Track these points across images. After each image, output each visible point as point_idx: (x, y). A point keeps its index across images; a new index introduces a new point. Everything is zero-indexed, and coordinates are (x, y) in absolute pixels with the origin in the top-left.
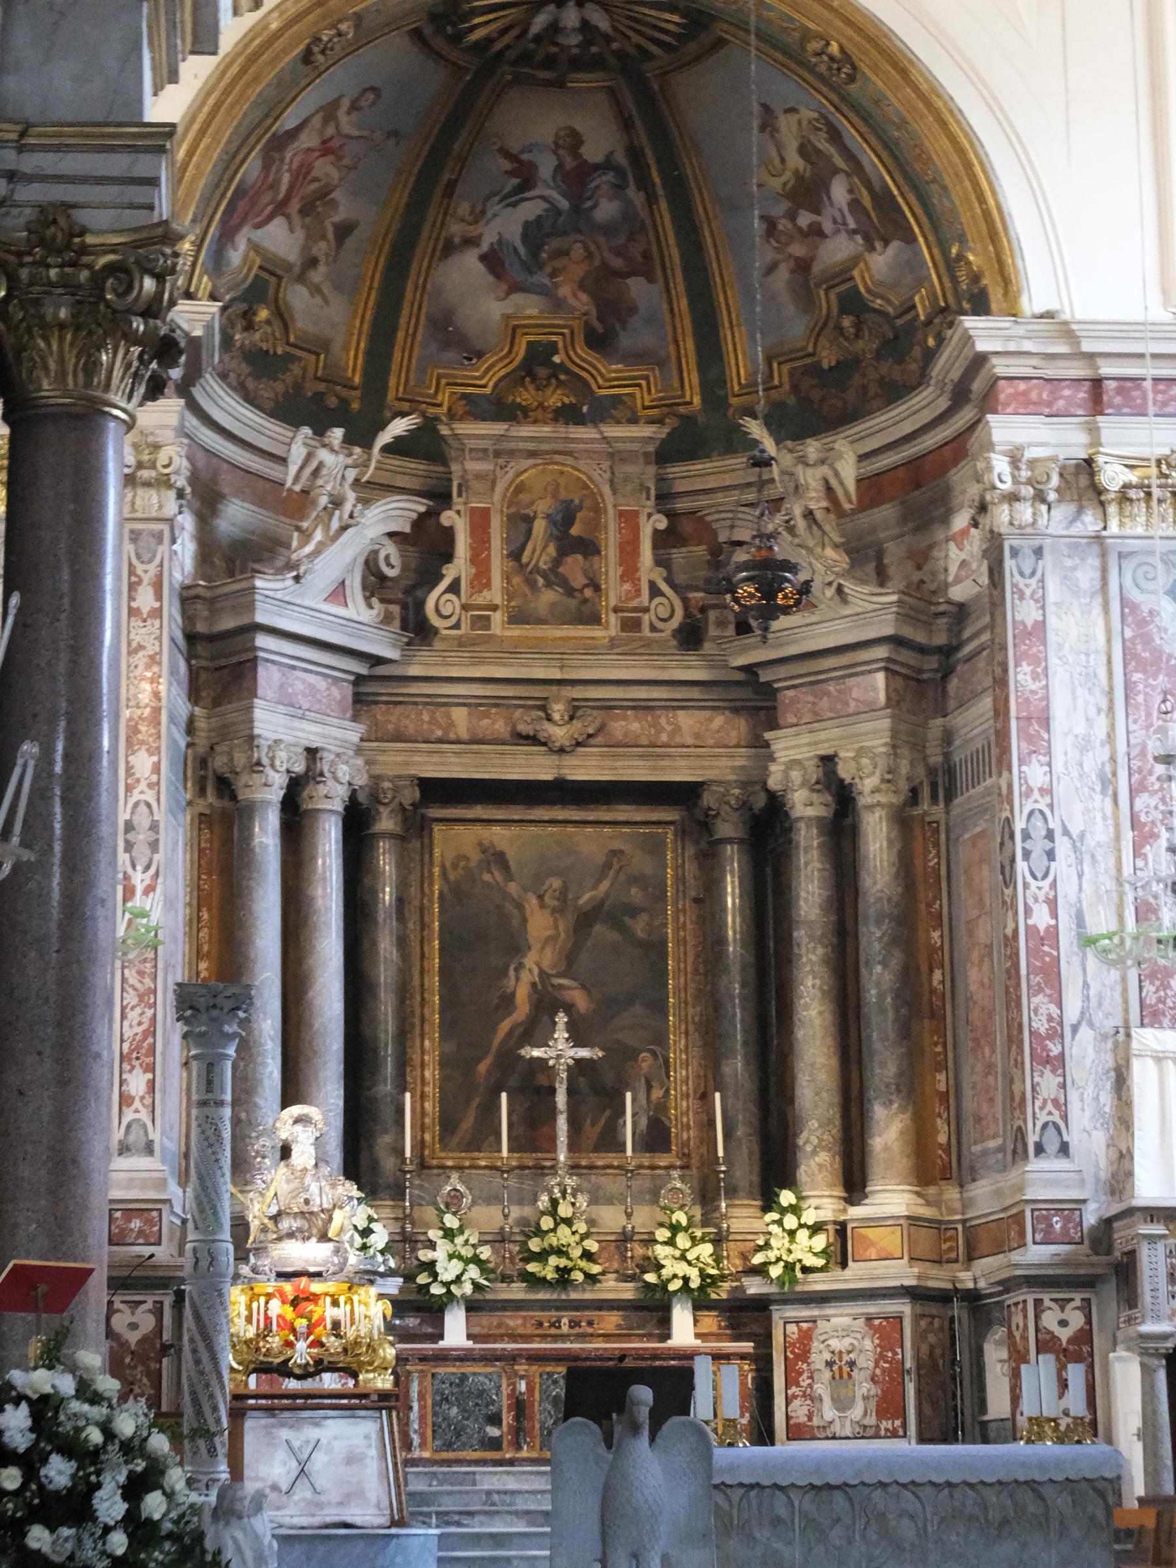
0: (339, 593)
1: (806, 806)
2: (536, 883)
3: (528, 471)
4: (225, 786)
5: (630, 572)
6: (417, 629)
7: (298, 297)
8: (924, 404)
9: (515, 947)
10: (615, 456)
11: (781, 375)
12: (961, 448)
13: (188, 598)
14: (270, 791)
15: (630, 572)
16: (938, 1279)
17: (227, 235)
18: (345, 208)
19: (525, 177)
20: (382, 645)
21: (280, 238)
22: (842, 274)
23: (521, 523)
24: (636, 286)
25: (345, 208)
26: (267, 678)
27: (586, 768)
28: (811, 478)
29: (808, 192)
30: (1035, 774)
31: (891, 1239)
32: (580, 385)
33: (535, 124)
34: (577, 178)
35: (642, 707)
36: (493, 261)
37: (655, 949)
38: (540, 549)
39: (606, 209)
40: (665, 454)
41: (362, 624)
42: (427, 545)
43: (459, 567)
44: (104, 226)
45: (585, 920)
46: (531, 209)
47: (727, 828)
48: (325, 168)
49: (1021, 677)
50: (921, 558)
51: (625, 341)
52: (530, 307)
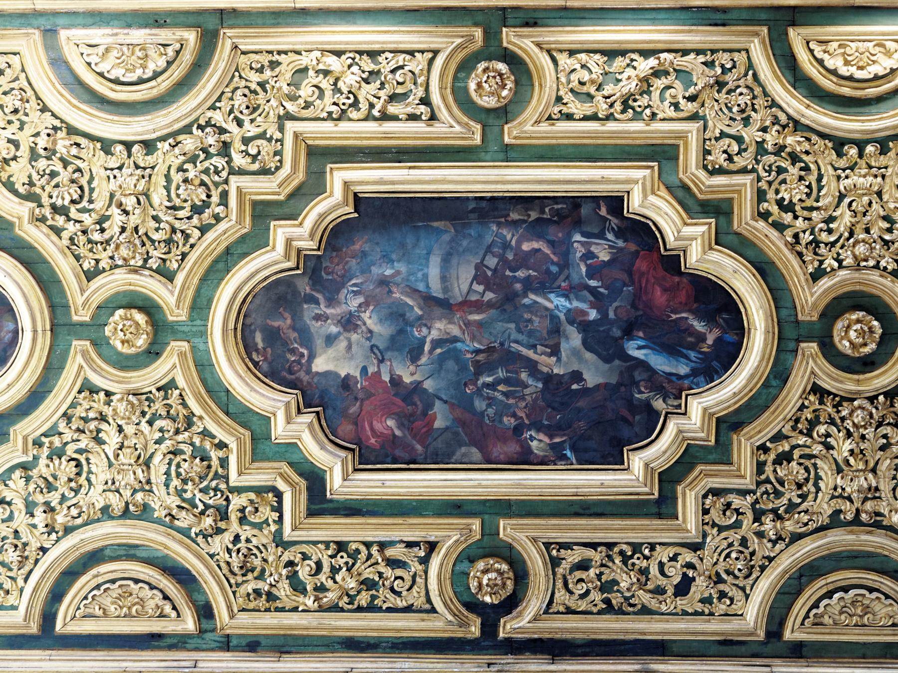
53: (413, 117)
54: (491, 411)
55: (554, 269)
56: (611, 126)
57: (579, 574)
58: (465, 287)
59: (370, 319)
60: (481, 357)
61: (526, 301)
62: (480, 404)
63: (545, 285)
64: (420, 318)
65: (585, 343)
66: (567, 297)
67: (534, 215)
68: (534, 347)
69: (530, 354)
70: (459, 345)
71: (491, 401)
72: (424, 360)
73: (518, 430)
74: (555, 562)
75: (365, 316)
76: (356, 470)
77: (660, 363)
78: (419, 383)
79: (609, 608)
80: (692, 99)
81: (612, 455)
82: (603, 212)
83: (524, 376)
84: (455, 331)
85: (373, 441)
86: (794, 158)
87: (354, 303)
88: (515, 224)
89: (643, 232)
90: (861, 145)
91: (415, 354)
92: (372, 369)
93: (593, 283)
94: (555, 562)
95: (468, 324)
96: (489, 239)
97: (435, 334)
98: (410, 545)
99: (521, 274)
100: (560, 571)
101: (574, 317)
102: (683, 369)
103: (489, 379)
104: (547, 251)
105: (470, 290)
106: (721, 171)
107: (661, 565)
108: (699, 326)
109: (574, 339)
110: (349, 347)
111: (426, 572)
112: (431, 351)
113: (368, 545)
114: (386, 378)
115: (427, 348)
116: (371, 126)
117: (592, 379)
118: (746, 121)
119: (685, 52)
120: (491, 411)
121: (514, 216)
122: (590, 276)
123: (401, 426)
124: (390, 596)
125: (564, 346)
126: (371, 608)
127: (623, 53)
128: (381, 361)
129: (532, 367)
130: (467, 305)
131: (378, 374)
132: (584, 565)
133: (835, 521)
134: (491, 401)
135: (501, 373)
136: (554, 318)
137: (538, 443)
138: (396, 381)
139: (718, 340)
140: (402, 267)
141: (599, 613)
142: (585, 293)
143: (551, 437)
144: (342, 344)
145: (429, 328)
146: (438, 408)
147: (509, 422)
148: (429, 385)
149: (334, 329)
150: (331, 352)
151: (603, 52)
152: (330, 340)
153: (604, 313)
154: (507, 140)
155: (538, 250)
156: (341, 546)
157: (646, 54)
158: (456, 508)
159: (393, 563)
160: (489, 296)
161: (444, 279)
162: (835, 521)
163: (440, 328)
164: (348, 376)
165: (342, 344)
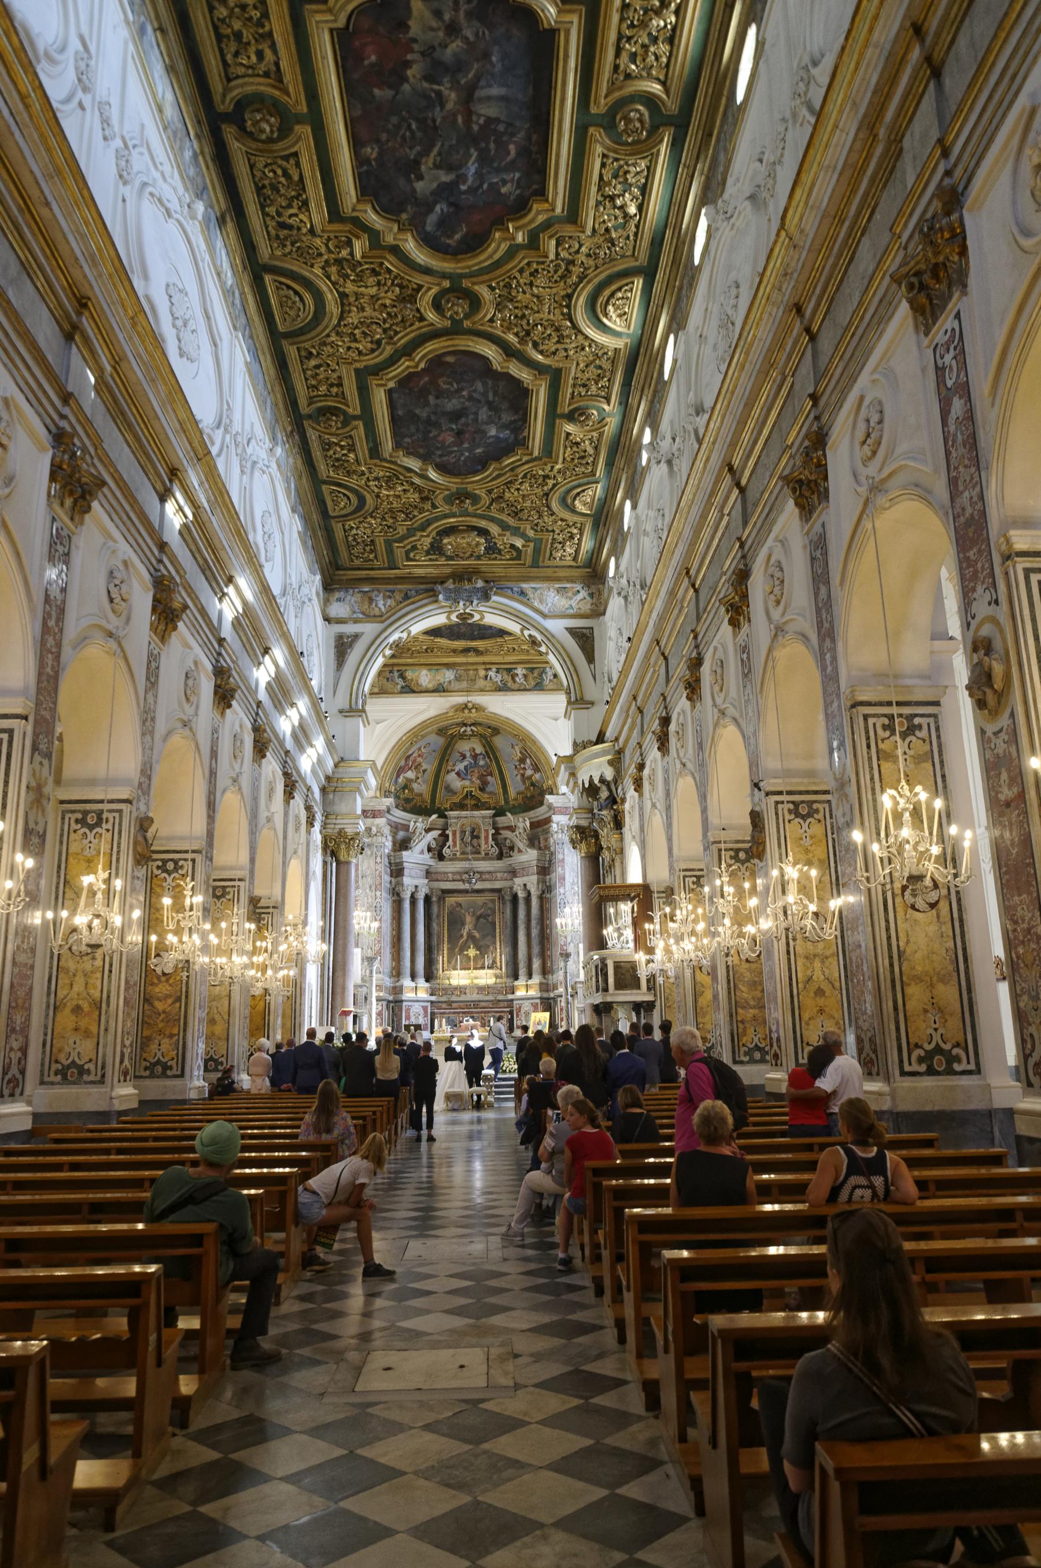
0: (422, 852)
1: (521, 895)
2: (467, 910)
3: (465, 821)
4: (398, 894)
5: (487, 843)
6: (441, 857)
7: (415, 786)
8: (543, 809)
9: (463, 924)
10: (484, 817)
11: (520, 797)
12: (548, 821)
13: (389, 856)
14: (407, 896)
15: (487, 843)
16: (545, 995)
17: (398, 776)
18: (424, 766)
19: (464, 757)
20: (432, 862)
21: (411, 775)
22: (530, 777)
23: (463, 832)
24: (489, 778)
25: (424, 766)
26: (406, 872)
27: (479, 886)
28: (521, 825)
29: (522, 761)
30: (562, 890)
31: (537, 987)
32: (479, 800)
33: (464, 746)
34: (475, 757)
35: (489, 872)
36: (458, 774)
37: (494, 924)
38: (468, 838)
39: (482, 763)
40: (495, 815)
41: (427, 859)
42: (444, 837)
43: (450, 843)
44: (350, 831)
45: (478, 918)
46: (465, 763)
47: (508, 898)
48: (419, 759)
49: (559, 870)
50: (546, 840)
51: (488, 789)
52: (467, 783)
53: (616, 68)
54: (390, 126)
55: (495, 165)
56: (594, 189)
57: (279, 172)
58: (482, 112)
59: (455, 46)
60: (430, 122)
61: (472, 150)
62: (394, 120)
63: (484, 159)
64: (458, 82)
65: (445, 183)
66: (476, 173)
67: (534, 149)
68: (439, 154)
69: (435, 151)
70: (438, 109)
71: (398, 127)
72: (426, 85)
73: (378, 141)
74: (286, 158)
75: (459, 42)
76: (331, 30)
77: (432, 219)
78: (406, 79)
79: (259, 189)
80: (607, 230)
81: (367, 188)
82: (535, 187)
83: (418, 148)
84: (450, 106)
85: (357, 43)
86: (562, 277)
87: (469, 33)
88: (529, 138)
89: (520, 208)
90: (568, 306)
91: (429, 78)
92: (416, 47)
93: (485, 186)
94: (286, 158)
95: (455, 115)
96: (518, 123)
97: (446, 92)
98: (277, 64)
99: (492, 146)
100: (280, 162)
101: (462, 178)
102: (428, 228)
103: (414, 127)
104: (509, 158)
105: (479, 116)
106: (558, 245)
107: (296, 215)
108: (457, 237)
109: (446, 178)
110: (432, 29)
111: (258, 75)
112: (432, 90)
113: (270, 34)
114: (409, 57)
115: (436, 87)
116: (612, 36)
117: (419, 186)
118: (589, 255)
119: (637, 227)
120: (390, 126)
121: (534, 137)
122: (491, 185)
123: (372, 65)
124: (233, 49)
125: (441, 172)
126: (219, 37)
127: (643, 194)
128: (423, 54)
129: (426, 153)
130: (469, 114)
131: (412, 51)
132: (286, 174)
133: (343, 296)
134: (398, 127)
135: (419, 134)
136: (460, 166)
137: (371, 152)
138: (408, 64)
139: (449, 245)
140: (499, 67)
141: (255, 183)
142: (478, 183)
143: (375, 160)
144: (434, 24)
145: (450, 89)
146: (389, 93)
147: (384, 137)
148: (406, 87)
149: (447, 17)
150: (427, 14)
151: (645, 185)
152: (438, 14)
153: (464, 193)
154: (591, 130)
155: (509, 154)
156: (265, 15)
157: (640, 208)
158: (313, 95)
159: (260, 55)
160: (476, 128)
161: (489, 98)
162: (343, 296)
163: (452, 97)
164: (408, 27)
165: (434, 24)
